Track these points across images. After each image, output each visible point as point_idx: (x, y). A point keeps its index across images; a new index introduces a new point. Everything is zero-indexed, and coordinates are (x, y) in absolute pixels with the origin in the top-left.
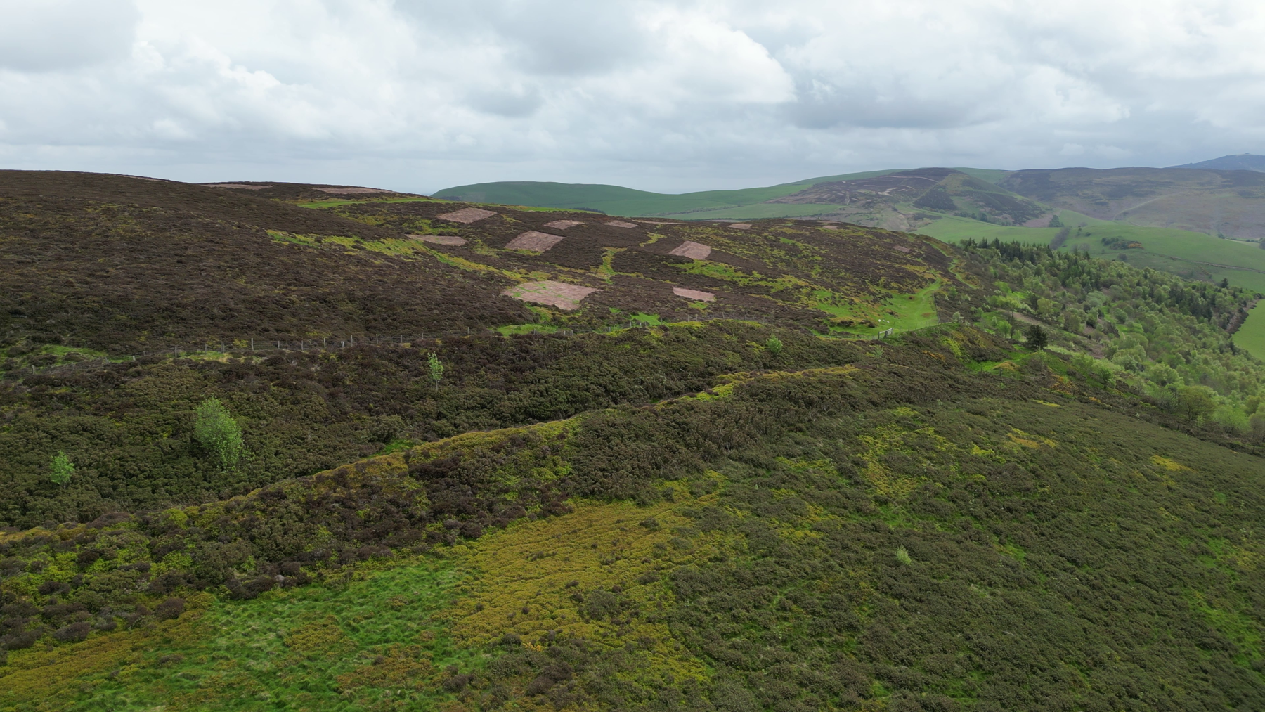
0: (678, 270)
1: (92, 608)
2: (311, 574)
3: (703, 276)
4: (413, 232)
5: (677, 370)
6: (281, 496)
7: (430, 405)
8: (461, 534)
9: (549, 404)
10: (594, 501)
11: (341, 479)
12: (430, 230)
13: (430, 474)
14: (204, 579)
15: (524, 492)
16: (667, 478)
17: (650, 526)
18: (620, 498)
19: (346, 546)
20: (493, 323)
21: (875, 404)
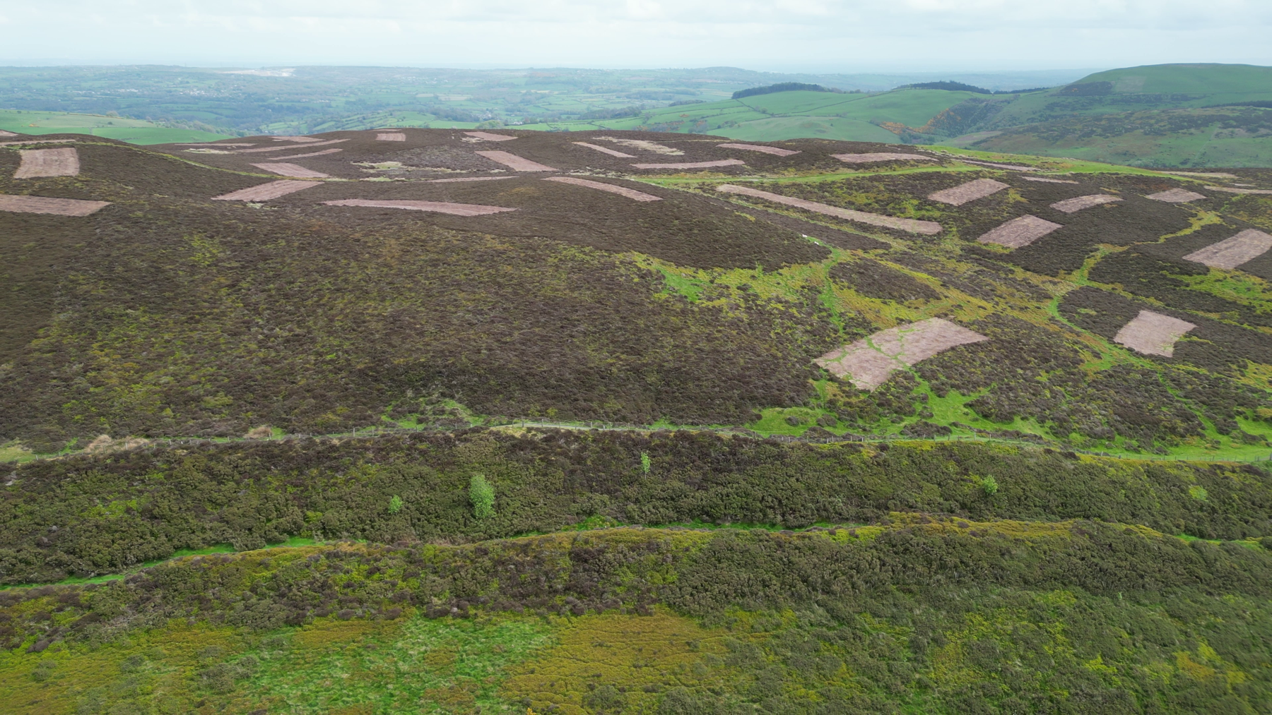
0: (1177, 283)
1: (361, 602)
2: (472, 612)
3: (1209, 294)
4: (895, 214)
5: (859, 495)
6: (486, 552)
7: (632, 491)
8: (571, 610)
9: (722, 507)
10: (672, 612)
11: (525, 549)
12: (913, 212)
13: (580, 557)
14: (417, 600)
15: (629, 590)
16: (742, 606)
17: (691, 646)
18: (691, 616)
19: (502, 599)
20: (761, 404)
21: (1026, 582)
